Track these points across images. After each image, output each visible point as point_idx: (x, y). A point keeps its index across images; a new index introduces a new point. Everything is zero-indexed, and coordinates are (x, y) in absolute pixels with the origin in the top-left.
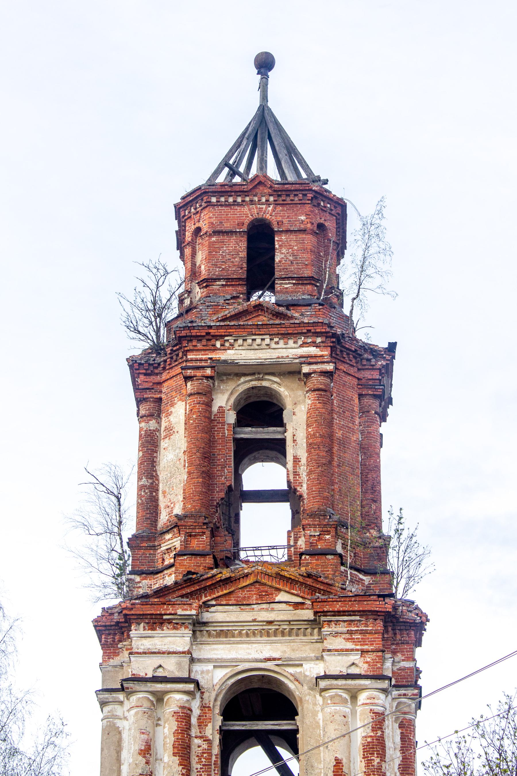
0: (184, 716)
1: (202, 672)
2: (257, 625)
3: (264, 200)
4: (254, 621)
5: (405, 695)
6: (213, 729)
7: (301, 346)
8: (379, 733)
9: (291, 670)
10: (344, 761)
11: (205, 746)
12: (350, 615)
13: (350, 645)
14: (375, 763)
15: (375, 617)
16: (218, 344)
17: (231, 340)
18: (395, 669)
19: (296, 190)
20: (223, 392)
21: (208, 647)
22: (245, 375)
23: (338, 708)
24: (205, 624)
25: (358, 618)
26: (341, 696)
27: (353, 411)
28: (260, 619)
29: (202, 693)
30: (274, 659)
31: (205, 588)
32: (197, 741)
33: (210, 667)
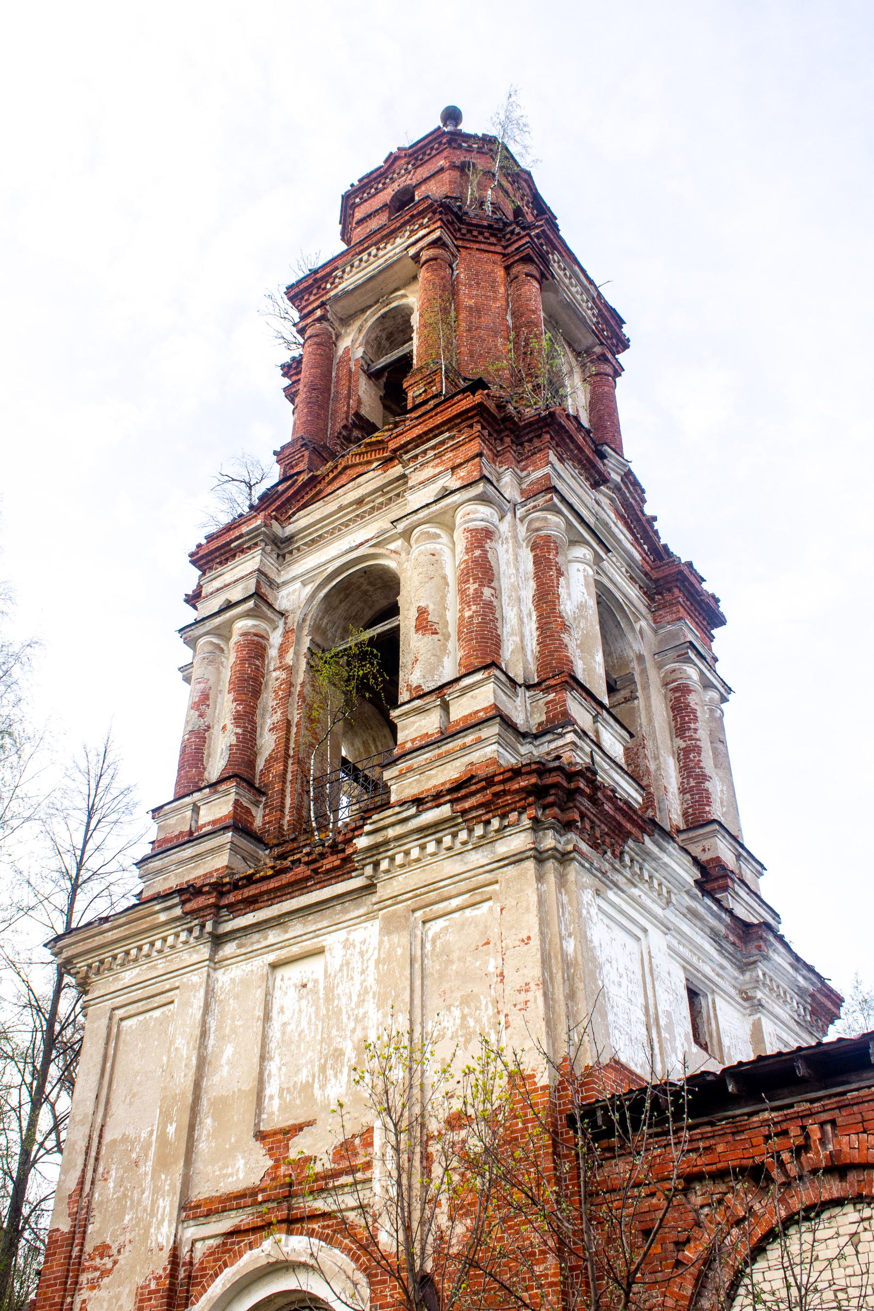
0: (255, 648)
1: (288, 595)
2: (348, 513)
3: (403, 172)
4: (341, 508)
5: (535, 507)
6: (296, 653)
7: (409, 238)
8: (477, 553)
9: (392, 546)
10: (431, 608)
11: (284, 676)
12: (436, 436)
13: (438, 470)
14: (471, 591)
15: (469, 422)
16: (329, 286)
17: (339, 273)
18: (524, 486)
19: (430, 142)
20: (349, 334)
21: (297, 565)
22: (370, 307)
23: (423, 548)
24: (290, 539)
25: (447, 435)
26: (428, 533)
27: (494, 281)
28: (346, 502)
29: (287, 618)
30: (367, 541)
31: (288, 500)
32: (274, 674)
33: (297, 585)
